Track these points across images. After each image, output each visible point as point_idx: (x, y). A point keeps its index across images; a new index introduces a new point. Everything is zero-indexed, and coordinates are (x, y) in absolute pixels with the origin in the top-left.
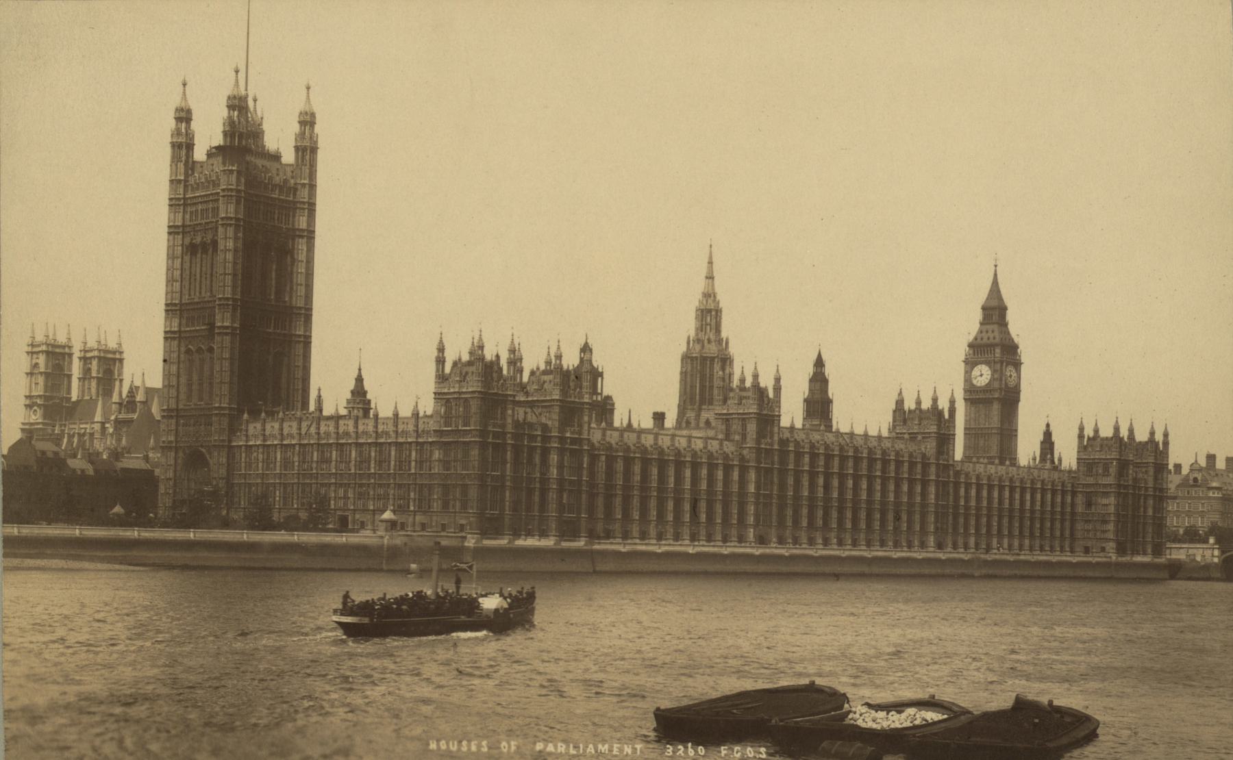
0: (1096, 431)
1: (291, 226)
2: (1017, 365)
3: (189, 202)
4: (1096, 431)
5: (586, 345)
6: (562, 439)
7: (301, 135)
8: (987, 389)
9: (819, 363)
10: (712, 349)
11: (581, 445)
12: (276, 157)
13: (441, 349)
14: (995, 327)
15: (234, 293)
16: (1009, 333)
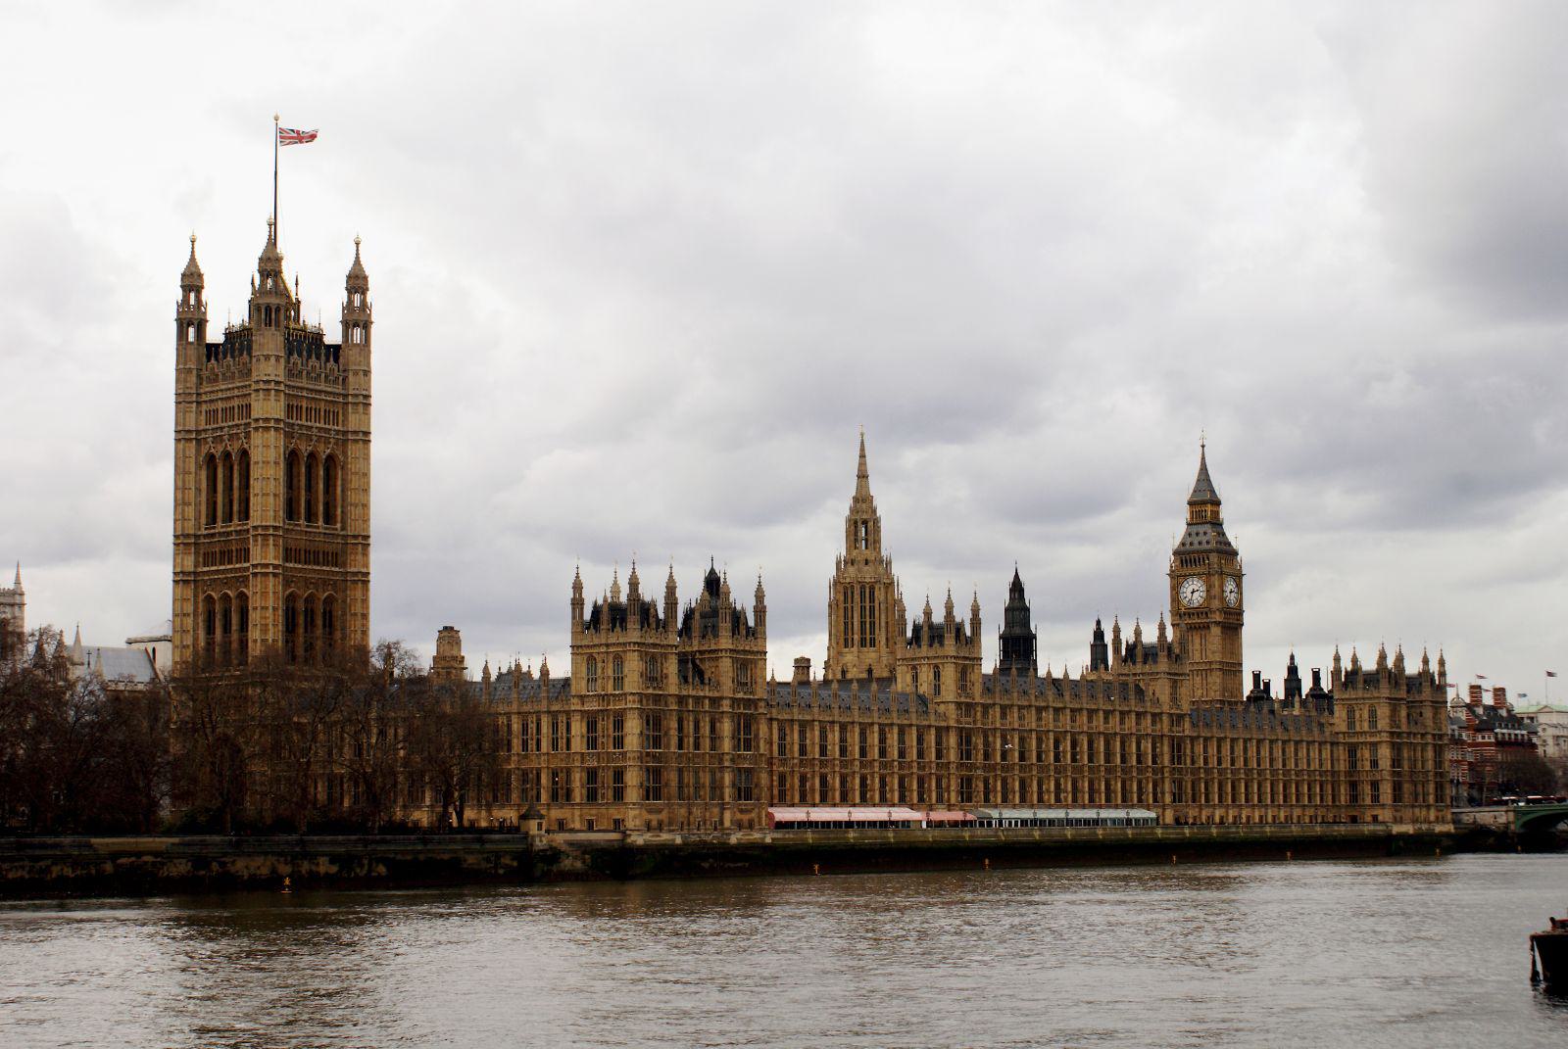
0: (1355, 660)
1: (340, 428)
2: (1238, 577)
3: (204, 398)
4: (1355, 660)
5: (712, 571)
7: (348, 307)
8: (1202, 611)
9: (1017, 588)
10: (868, 574)
11: (756, 708)
12: (318, 336)
13: (578, 587)
14: (1208, 528)
15: (275, 519)
16: (1224, 534)
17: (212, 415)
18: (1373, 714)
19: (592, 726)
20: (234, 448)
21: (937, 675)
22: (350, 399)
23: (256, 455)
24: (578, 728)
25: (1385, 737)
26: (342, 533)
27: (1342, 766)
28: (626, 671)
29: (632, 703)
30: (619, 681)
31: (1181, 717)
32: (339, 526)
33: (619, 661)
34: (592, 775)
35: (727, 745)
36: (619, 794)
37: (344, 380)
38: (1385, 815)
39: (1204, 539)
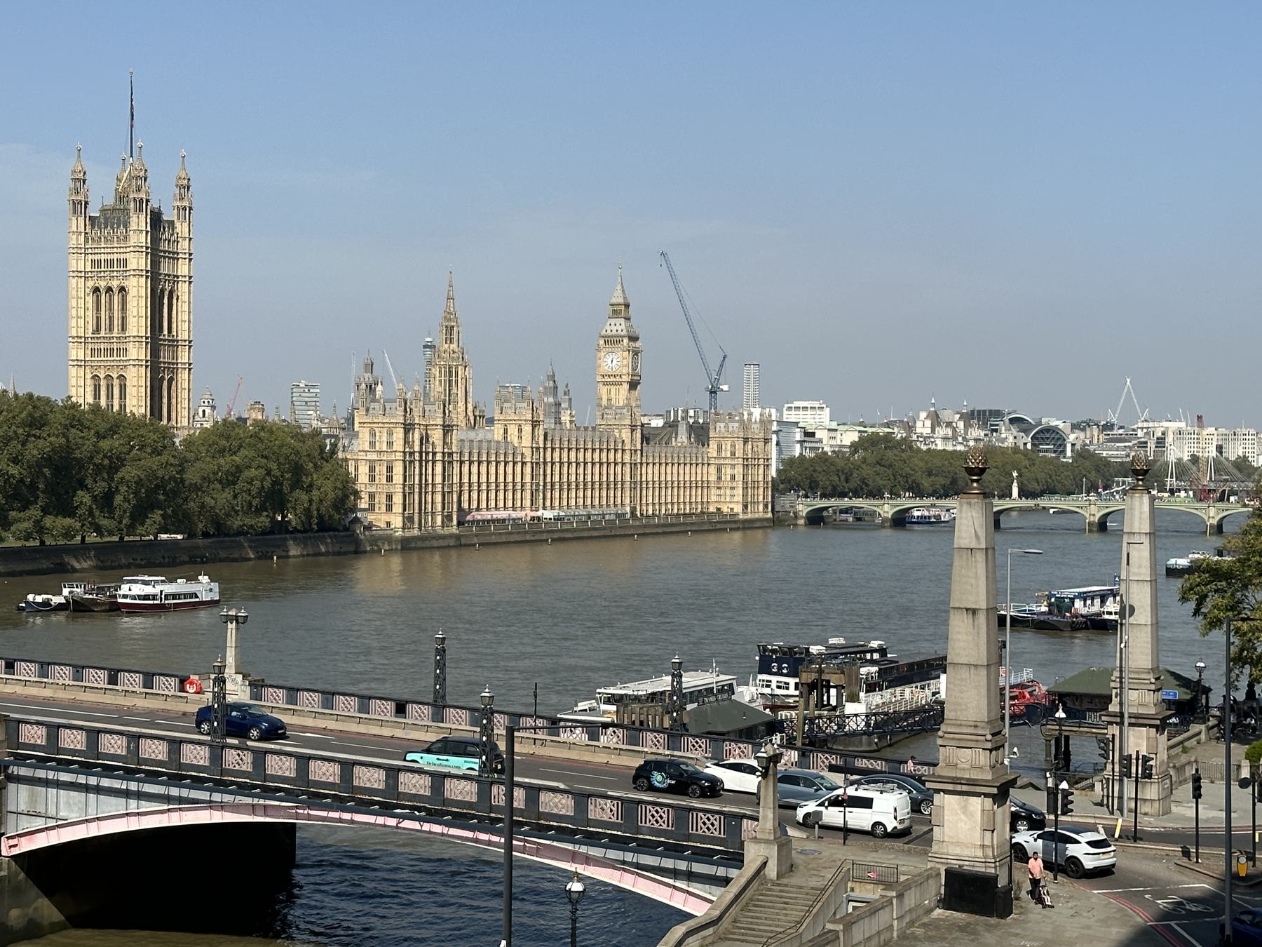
3: (90, 251)
6: (443, 453)
14: (622, 321)
15: (146, 333)
17: (96, 263)
18: (733, 446)
19: (372, 469)
20: (115, 284)
21: (520, 430)
22: (180, 256)
23: (132, 292)
24: (364, 470)
25: (741, 461)
26: (179, 338)
27: (713, 478)
28: (395, 439)
29: (400, 456)
30: (390, 444)
31: (636, 451)
32: (175, 334)
33: (390, 433)
34: (372, 496)
35: (439, 479)
36: (389, 508)
37: (178, 242)
38: (738, 509)
39: (620, 329)
